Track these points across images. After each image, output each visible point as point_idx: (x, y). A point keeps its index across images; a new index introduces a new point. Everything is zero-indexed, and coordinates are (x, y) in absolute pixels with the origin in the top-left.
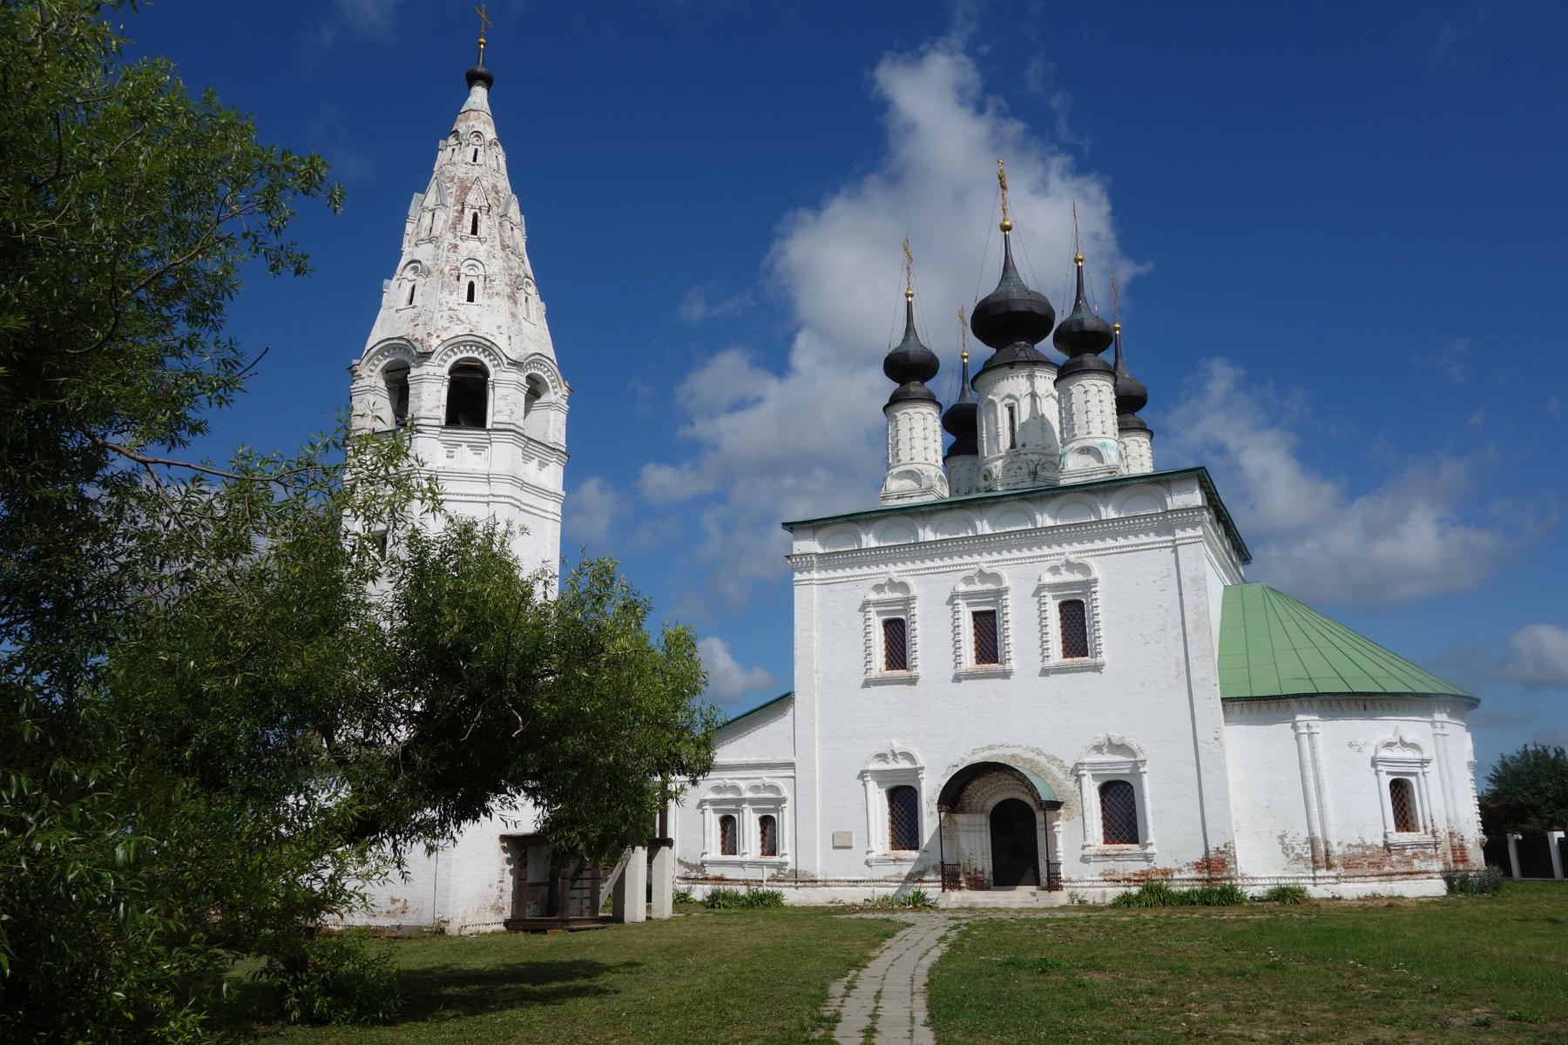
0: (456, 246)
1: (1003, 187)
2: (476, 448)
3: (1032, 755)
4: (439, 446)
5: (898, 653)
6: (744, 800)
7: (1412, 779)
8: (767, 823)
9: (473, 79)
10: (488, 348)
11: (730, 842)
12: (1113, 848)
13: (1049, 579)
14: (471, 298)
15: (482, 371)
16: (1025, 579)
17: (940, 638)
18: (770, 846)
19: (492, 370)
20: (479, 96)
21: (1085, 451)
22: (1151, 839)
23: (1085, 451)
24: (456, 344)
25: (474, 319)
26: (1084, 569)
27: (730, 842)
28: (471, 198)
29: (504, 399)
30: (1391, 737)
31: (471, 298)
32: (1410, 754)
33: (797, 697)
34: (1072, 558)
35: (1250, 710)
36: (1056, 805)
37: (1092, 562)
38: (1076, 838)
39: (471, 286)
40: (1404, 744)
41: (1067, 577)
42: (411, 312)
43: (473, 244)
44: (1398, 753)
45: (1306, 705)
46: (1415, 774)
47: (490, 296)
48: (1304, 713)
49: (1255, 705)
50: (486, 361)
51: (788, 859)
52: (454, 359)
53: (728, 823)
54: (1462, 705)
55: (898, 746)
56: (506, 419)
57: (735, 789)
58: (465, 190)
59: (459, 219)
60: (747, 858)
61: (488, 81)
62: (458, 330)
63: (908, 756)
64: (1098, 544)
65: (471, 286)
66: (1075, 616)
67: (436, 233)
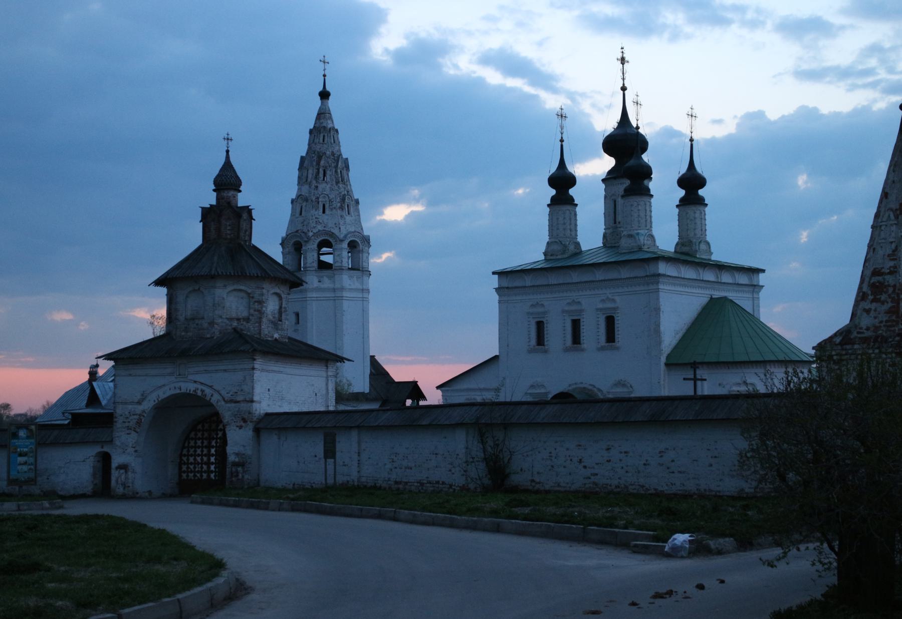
0: (317, 187)
1: (623, 60)
2: (330, 278)
3: (590, 387)
5: (540, 340)
10: (332, 235)
13: (601, 306)
14: (324, 212)
16: (592, 306)
17: (558, 332)
21: (630, 236)
23: (630, 236)
25: (325, 221)
26: (614, 301)
28: (322, 163)
30: (739, 380)
31: (324, 212)
34: (610, 296)
37: (617, 298)
39: (324, 206)
41: (609, 305)
42: (301, 219)
43: (324, 185)
47: (332, 210)
58: (320, 158)
59: (318, 173)
62: (320, 227)
63: (543, 386)
64: (620, 290)
65: (324, 206)
67: (309, 180)
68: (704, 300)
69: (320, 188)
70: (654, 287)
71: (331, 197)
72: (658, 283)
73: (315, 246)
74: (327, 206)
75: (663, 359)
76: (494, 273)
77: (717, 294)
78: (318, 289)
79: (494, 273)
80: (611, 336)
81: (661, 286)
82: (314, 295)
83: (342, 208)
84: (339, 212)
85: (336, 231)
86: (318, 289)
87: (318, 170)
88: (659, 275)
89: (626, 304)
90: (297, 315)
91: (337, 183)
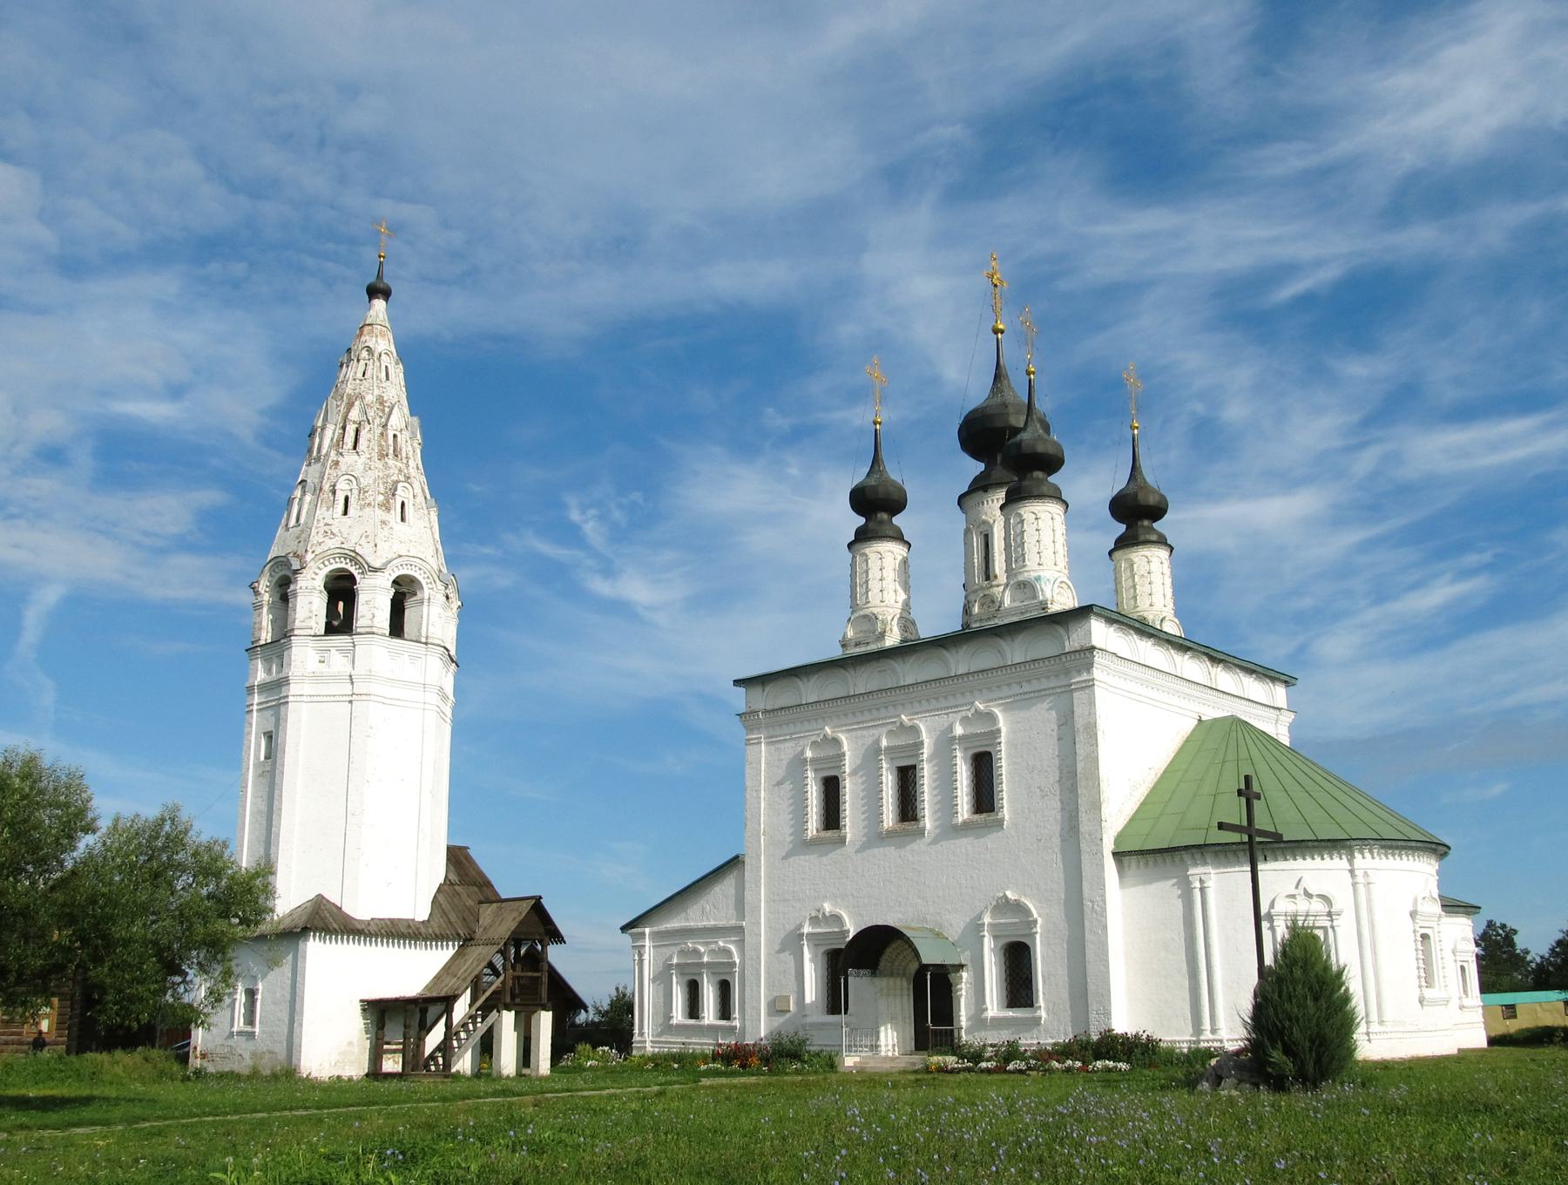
0: (337, 463)
4: (310, 651)
6: (701, 965)
7: (1320, 933)
8: (725, 989)
9: (374, 292)
10: (354, 558)
11: (694, 1009)
12: (1010, 1013)
15: (351, 578)
18: (725, 1011)
19: (358, 578)
20: (379, 304)
22: (1041, 1000)
24: (324, 558)
27: (694, 1009)
28: (355, 414)
29: (373, 603)
32: (1317, 906)
33: (747, 860)
35: (1147, 864)
36: (961, 966)
38: (980, 1001)
39: (347, 499)
40: (1308, 895)
43: (349, 459)
44: (1302, 906)
45: (1198, 856)
46: (1324, 928)
48: (1196, 865)
49: (1150, 858)
50: (353, 570)
51: (737, 1023)
52: (326, 570)
53: (693, 990)
54: (1438, 849)
55: (827, 907)
56: (369, 623)
57: (696, 951)
58: (350, 405)
60: (706, 1022)
61: (386, 294)
62: (331, 543)
66: (983, 765)
68: (1190, 725)
69: (343, 467)
70: (1085, 677)
71: (364, 482)
72: (1089, 666)
73: (319, 582)
74: (352, 501)
75: (1108, 846)
76: (737, 682)
77: (1210, 713)
78: (316, 678)
79: (737, 682)
80: (984, 798)
81: (1097, 673)
82: (307, 689)
83: (386, 506)
84: (380, 514)
85: (365, 551)
86: (316, 678)
87: (344, 428)
88: (1093, 648)
89: (1018, 734)
90: (269, 736)
91: (382, 456)
